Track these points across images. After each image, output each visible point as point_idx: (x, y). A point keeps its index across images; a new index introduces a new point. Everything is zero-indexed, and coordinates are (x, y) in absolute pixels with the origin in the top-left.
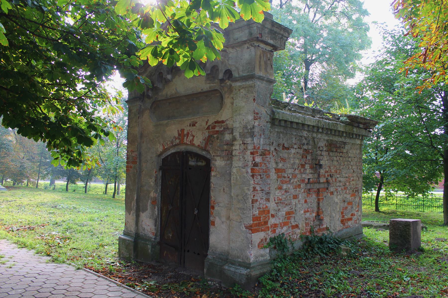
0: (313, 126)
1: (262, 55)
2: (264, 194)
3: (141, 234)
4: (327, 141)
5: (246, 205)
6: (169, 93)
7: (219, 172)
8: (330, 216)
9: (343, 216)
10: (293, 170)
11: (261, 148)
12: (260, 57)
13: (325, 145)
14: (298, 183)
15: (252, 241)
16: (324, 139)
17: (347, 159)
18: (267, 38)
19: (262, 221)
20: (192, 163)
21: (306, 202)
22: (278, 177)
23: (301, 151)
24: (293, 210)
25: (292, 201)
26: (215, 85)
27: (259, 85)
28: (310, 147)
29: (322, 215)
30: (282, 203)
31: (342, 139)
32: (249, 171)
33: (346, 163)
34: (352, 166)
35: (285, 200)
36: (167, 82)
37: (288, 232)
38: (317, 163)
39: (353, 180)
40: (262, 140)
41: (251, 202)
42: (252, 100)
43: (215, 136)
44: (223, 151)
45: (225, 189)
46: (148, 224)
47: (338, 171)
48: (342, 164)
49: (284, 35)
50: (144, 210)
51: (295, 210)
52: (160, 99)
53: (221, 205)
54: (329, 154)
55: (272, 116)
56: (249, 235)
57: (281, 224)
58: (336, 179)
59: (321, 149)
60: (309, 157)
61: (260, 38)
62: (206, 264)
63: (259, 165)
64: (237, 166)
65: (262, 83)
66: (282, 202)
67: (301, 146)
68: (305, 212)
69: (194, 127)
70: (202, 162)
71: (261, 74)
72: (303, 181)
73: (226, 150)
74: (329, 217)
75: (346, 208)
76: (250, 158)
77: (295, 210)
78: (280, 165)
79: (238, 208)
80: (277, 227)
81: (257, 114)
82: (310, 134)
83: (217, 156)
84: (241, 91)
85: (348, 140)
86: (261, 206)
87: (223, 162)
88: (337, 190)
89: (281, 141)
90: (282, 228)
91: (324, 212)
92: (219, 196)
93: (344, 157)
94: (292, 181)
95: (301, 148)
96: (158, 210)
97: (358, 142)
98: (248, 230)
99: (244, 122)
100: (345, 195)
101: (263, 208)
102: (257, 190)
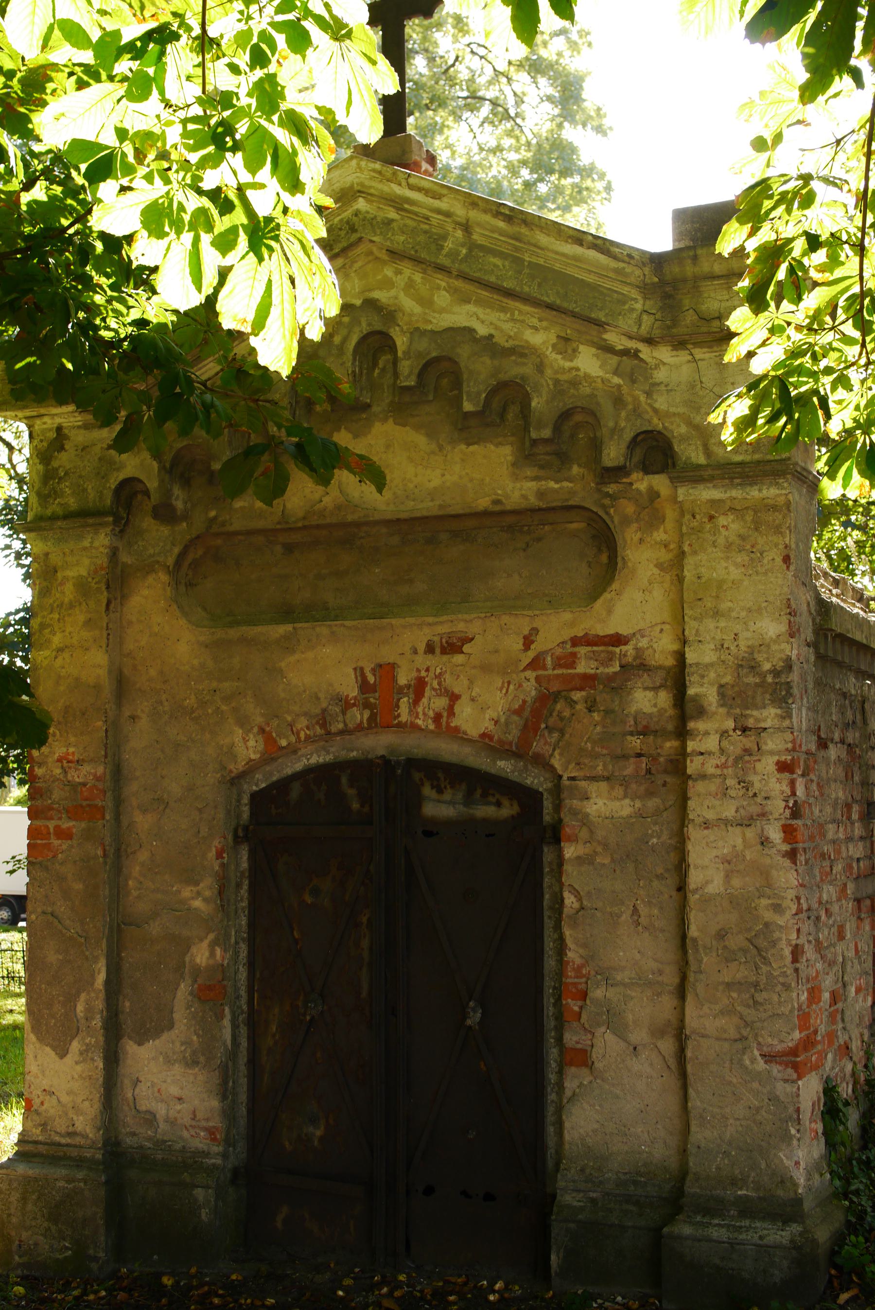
5: (764, 969)
7: (606, 846)
20: (440, 807)
32: (775, 835)
41: (789, 958)
43: (577, 696)
44: (625, 757)
45: (643, 910)
46: (174, 1091)
52: (237, 525)
64: (710, 815)
69: (459, 659)
70: (499, 804)
83: (594, 779)
84: (722, 521)
87: (627, 801)
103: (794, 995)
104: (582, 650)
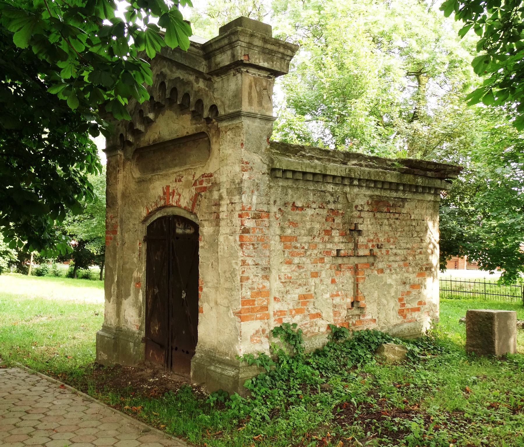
0: (343, 178)
1: (253, 83)
2: (259, 270)
3: (123, 328)
4: (371, 197)
6: (152, 139)
8: (379, 304)
9: (403, 305)
10: (310, 238)
11: (253, 209)
12: (250, 87)
13: (368, 203)
14: (321, 256)
15: (241, 332)
16: (365, 195)
17: (409, 222)
18: (257, 61)
19: (256, 305)
21: (333, 281)
22: (286, 247)
23: (325, 212)
24: (312, 292)
25: (310, 280)
26: (201, 127)
27: (248, 125)
28: (340, 206)
29: (363, 302)
30: (293, 283)
31: (400, 195)
32: (238, 239)
33: (406, 228)
34: (418, 232)
35: (297, 279)
36: (148, 123)
37: (303, 323)
38: (353, 227)
39: (421, 253)
40: (254, 198)
42: (240, 146)
45: (214, 264)
46: (131, 314)
47: (392, 240)
48: (400, 230)
49: (286, 53)
50: (127, 295)
51: (315, 293)
53: (210, 285)
54: (374, 215)
55: (270, 165)
56: (238, 324)
57: (291, 311)
58: (388, 251)
59: (360, 208)
60: (338, 220)
61: (245, 62)
62: (193, 364)
63: (251, 231)
65: (254, 122)
66: (292, 281)
67: (324, 205)
68: (332, 296)
70: (190, 229)
71: (255, 109)
72: (328, 253)
73: (215, 212)
74: (376, 304)
75: (409, 293)
76: (237, 221)
77: (315, 293)
78: (289, 232)
79: (226, 288)
80: (285, 314)
81: (247, 163)
82: (338, 189)
83: (205, 220)
85: (408, 196)
86: (255, 286)
88: (390, 266)
89: (289, 199)
90: (293, 317)
91: (366, 297)
92: (207, 275)
93: (403, 220)
94: (308, 253)
95: (324, 208)
96: (143, 294)
97: (431, 198)
98: (236, 317)
99: (232, 174)
100: (406, 275)
101: (258, 288)
102: (248, 265)
103: (240, 293)
104: (204, 179)
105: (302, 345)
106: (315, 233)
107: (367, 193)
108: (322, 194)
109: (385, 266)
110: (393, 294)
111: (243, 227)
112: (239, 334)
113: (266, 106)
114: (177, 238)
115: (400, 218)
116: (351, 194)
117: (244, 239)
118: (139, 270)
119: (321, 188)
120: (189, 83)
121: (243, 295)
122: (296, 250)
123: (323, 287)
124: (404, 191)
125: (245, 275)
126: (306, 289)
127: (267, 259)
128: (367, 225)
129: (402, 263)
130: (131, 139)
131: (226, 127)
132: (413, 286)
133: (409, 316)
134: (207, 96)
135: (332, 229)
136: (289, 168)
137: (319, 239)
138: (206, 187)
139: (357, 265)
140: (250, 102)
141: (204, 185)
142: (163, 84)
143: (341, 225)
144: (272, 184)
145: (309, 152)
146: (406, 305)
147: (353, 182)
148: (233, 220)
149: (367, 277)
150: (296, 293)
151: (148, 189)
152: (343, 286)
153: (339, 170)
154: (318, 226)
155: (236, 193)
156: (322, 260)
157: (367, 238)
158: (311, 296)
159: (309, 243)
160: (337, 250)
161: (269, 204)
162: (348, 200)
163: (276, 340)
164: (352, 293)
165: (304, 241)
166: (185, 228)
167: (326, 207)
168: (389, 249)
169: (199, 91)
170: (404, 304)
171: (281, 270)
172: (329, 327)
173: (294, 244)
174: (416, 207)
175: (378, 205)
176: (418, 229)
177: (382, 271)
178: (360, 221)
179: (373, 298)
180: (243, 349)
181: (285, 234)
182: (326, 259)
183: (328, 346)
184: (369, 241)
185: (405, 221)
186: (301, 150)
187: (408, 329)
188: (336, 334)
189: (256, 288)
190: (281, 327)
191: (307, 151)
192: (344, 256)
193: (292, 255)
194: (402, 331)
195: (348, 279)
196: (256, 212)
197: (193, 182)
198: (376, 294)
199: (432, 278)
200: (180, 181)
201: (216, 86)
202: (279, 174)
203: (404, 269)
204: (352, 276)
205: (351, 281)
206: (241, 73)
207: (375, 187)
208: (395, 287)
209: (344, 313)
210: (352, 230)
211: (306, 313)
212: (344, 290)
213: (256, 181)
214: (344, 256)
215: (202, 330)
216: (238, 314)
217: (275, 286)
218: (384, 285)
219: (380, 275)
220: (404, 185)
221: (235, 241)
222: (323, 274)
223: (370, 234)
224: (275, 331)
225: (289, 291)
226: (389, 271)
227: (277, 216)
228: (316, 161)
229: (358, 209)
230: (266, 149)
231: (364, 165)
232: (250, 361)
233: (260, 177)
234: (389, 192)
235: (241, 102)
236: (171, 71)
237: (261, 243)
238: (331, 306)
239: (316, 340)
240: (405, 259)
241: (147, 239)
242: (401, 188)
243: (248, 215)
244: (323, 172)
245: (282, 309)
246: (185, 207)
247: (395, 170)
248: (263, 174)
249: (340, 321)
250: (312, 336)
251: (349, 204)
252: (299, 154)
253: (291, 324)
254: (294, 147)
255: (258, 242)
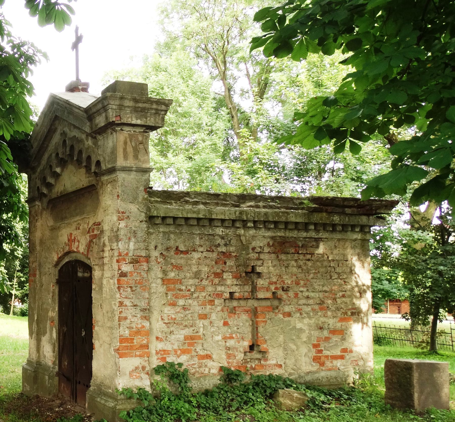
0: (234, 221)
1: (128, 140)
2: (138, 311)
4: (272, 238)
8: (285, 349)
9: (321, 351)
10: (197, 281)
11: (131, 254)
12: (125, 143)
14: (210, 298)
16: (264, 237)
19: (135, 344)
21: (226, 324)
22: (169, 290)
23: (215, 255)
24: (200, 334)
25: (198, 322)
27: (124, 178)
28: (232, 249)
29: (265, 346)
30: (177, 324)
31: (313, 234)
32: (116, 282)
33: (322, 270)
34: (339, 274)
35: (182, 320)
37: (190, 363)
39: (343, 296)
40: (132, 244)
47: (302, 283)
48: (314, 271)
51: (204, 335)
54: (278, 257)
55: (148, 213)
56: (117, 359)
57: (175, 351)
58: (296, 295)
65: (130, 175)
66: (176, 322)
67: (214, 248)
72: (219, 295)
76: (115, 266)
77: (204, 335)
78: (172, 275)
80: (169, 354)
81: (123, 213)
82: (230, 232)
85: (322, 235)
86: (134, 325)
89: (172, 243)
90: (179, 357)
91: (269, 342)
94: (195, 295)
95: (213, 251)
98: (116, 354)
100: (323, 319)
102: (126, 306)
105: (189, 384)
106: (203, 276)
107: (266, 235)
108: (211, 237)
109: (294, 309)
110: (305, 339)
111: (120, 271)
112: (118, 369)
113: (142, 159)
114: (79, 281)
115: (312, 258)
116: (246, 236)
117: (121, 282)
118: (53, 310)
119: (208, 232)
120: (80, 141)
121: (121, 333)
122: (181, 292)
123: (212, 329)
124: (317, 230)
125: (123, 315)
126: (194, 330)
127: (147, 301)
128: (268, 266)
129: (317, 307)
130: (45, 191)
131: (107, 180)
132: (334, 332)
133: (328, 364)
134: (94, 152)
135: (223, 271)
136: (167, 215)
137: (207, 281)
138: (95, 234)
139: (256, 308)
140: (126, 157)
141: (96, 232)
142: (65, 141)
143: (235, 267)
144: (151, 230)
145: (195, 197)
146: (324, 352)
147: (247, 224)
148: (113, 265)
149: (269, 321)
150: (180, 334)
151: (58, 236)
152: (238, 329)
153: (227, 213)
154: (206, 269)
155: (114, 240)
156: (211, 302)
157: (268, 280)
158: (199, 338)
159: (196, 286)
160: (230, 293)
161: (147, 249)
162: (242, 242)
163: (158, 378)
164: (250, 336)
165: (190, 283)
166: (84, 272)
167: (215, 250)
168: (299, 292)
169: (88, 148)
170: (322, 350)
171: (162, 312)
172: (221, 369)
173: (178, 286)
174: (336, 247)
175: (280, 247)
176: (338, 270)
177: (289, 315)
178: (259, 263)
179: (277, 342)
180: (122, 383)
181: (168, 277)
182: (217, 302)
183: (218, 388)
184: (271, 283)
185: (320, 262)
186: (185, 197)
187: (327, 378)
188: (229, 376)
189: (134, 327)
190: (163, 365)
191: (193, 196)
192: (240, 299)
193: (176, 298)
194: (318, 379)
195: (244, 322)
196: (134, 257)
197: (88, 229)
198: (281, 338)
199: (360, 324)
200: (79, 229)
201: (99, 143)
202: (159, 221)
203: (320, 314)
204: (249, 319)
205: (248, 324)
206: (116, 131)
207: (276, 227)
208: (307, 332)
209: (240, 356)
210: (250, 273)
211: (194, 353)
212: (240, 333)
213: (134, 228)
214: (240, 299)
215: (95, 365)
216: (117, 350)
217: (158, 327)
218: (291, 330)
219: (287, 319)
220: (315, 225)
221: (115, 284)
222: (214, 317)
223: (272, 276)
224: (157, 368)
225: (173, 331)
226: (299, 314)
227: (158, 260)
228: (201, 207)
229: (256, 251)
230: (144, 199)
231: (261, 206)
232: (128, 394)
233: (137, 224)
234: (296, 232)
235: (116, 158)
236: (70, 130)
237: (139, 286)
238: (224, 349)
239: (205, 380)
240: (322, 303)
241: (59, 282)
242: (312, 227)
243: (124, 260)
244: (208, 217)
245: (165, 348)
246: (83, 253)
247: (303, 209)
248: (141, 222)
249: (235, 364)
250: (201, 377)
251: (244, 247)
252: (182, 200)
253: (176, 363)
254: (178, 194)
255: (136, 285)
